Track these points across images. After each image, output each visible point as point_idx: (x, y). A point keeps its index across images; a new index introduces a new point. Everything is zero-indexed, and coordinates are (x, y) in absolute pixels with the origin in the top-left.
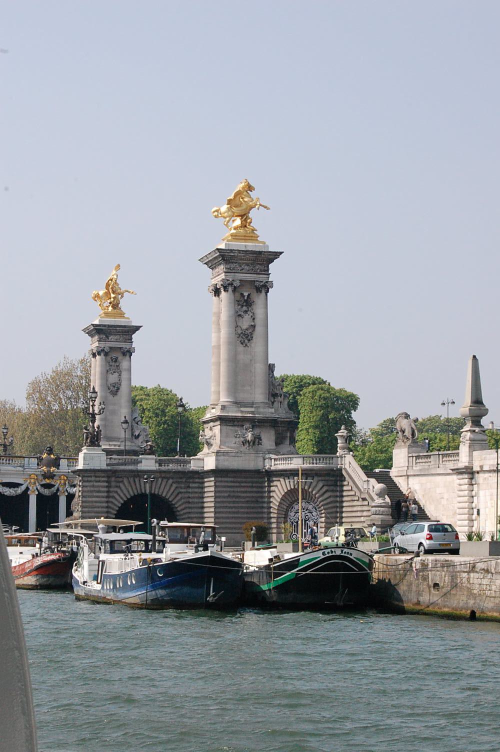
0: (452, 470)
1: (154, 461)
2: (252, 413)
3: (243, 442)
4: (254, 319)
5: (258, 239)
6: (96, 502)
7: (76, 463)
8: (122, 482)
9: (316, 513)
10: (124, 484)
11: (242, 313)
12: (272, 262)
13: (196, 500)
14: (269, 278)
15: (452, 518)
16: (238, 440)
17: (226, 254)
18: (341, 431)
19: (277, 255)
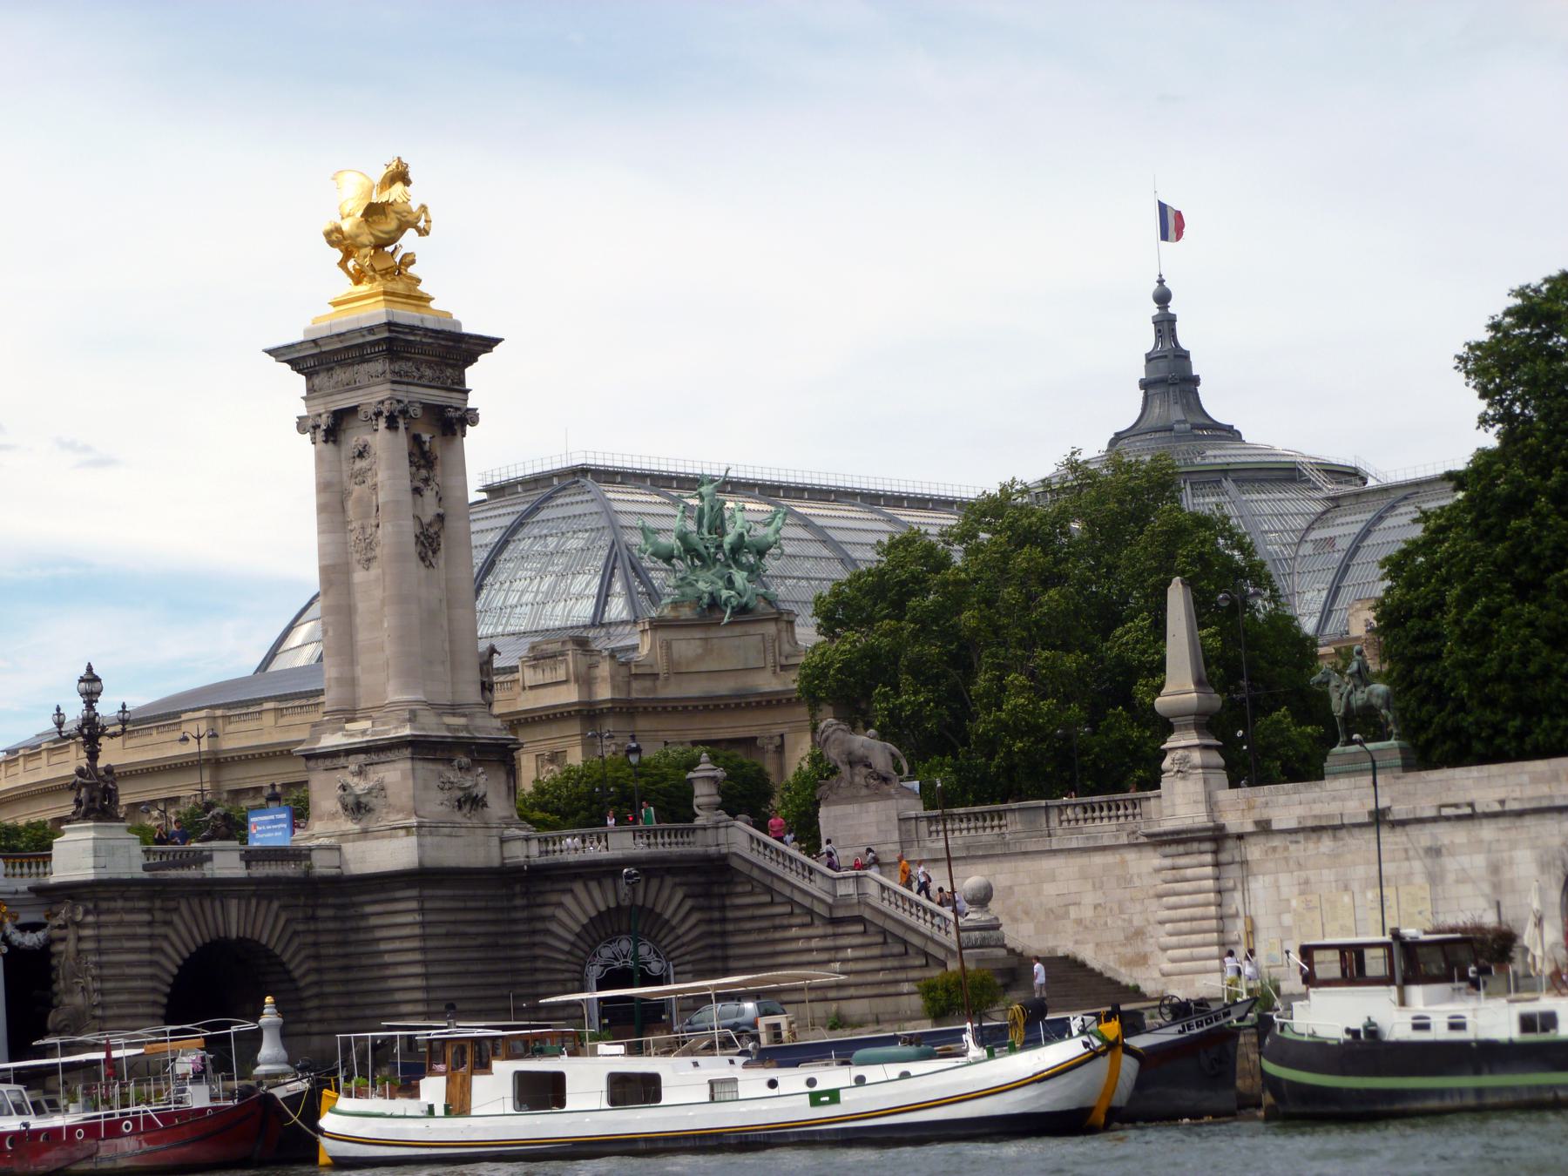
0: (1147, 836)
1: (236, 855)
2: (466, 728)
3: (459, 801)
4: (440, 499)
5: (433, 304)
6: (130, 964)
7: (45, 867)
8: (176, 910)
9: (660, 965)
10: (182, 917)
11: (421, 485)
12: (471, 364)
13: (332, 951)
14: (466, 400)
15: (1125, 945)
16: (447, 794)
17: (402, 336)
18: (700, 767)
19: (488, 344)
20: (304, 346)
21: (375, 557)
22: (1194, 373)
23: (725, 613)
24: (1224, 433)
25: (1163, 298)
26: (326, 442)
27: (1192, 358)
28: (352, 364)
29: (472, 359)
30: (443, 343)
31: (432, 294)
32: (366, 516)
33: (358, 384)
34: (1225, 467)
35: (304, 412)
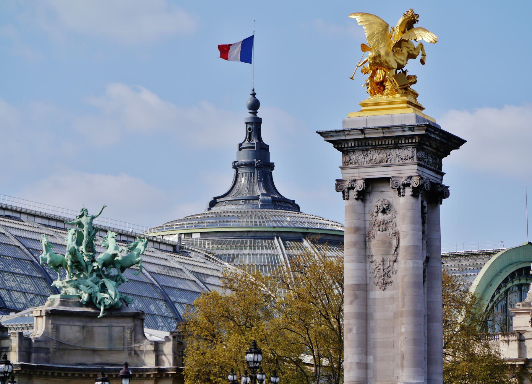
5: (423, 112)
14: (442, 180)
20: (351, 133)
21: (391, 282)
22: (271, 161)
23: (100, 309)
24: (291, 206)
25: (255, 106)
26: (357, 199)
27: (270, 150)
28: (385, 149)
29: (447, 153)
30: (443, 140)
31: (423, 106)
32: (388, 253)
33: (389, 163)
34: (305, 231)
35: (341, 178)
